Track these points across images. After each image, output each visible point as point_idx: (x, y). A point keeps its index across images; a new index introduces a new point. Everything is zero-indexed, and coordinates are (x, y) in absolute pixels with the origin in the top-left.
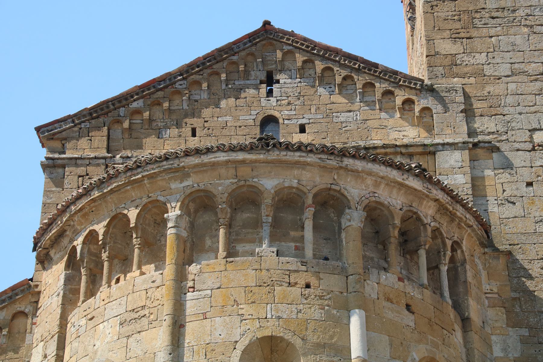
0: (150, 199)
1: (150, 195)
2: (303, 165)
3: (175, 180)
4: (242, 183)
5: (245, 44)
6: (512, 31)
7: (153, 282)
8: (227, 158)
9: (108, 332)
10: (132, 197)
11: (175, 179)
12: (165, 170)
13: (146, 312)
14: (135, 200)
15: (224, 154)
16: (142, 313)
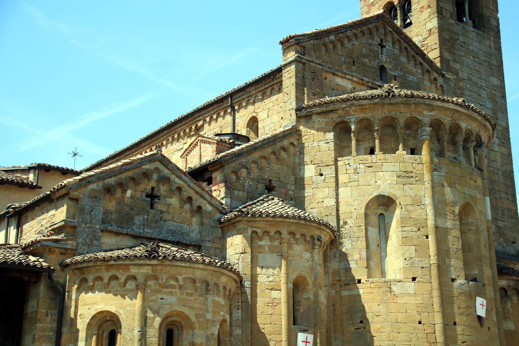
0: (411, 116)
1: (412, 113)
2: (475, 119)
3: (427, 110)
4: (454, 121)
5: (374, 20)
6: (468, 56)
7: (416, 160)
8: (454, 107)
9: (387, 178)
10: (401, 111)
11: (427, 110)
12: (426, 104)
13: (414, 175)
14: (403, 113)
15: (453, 105)
16: (411, 175)
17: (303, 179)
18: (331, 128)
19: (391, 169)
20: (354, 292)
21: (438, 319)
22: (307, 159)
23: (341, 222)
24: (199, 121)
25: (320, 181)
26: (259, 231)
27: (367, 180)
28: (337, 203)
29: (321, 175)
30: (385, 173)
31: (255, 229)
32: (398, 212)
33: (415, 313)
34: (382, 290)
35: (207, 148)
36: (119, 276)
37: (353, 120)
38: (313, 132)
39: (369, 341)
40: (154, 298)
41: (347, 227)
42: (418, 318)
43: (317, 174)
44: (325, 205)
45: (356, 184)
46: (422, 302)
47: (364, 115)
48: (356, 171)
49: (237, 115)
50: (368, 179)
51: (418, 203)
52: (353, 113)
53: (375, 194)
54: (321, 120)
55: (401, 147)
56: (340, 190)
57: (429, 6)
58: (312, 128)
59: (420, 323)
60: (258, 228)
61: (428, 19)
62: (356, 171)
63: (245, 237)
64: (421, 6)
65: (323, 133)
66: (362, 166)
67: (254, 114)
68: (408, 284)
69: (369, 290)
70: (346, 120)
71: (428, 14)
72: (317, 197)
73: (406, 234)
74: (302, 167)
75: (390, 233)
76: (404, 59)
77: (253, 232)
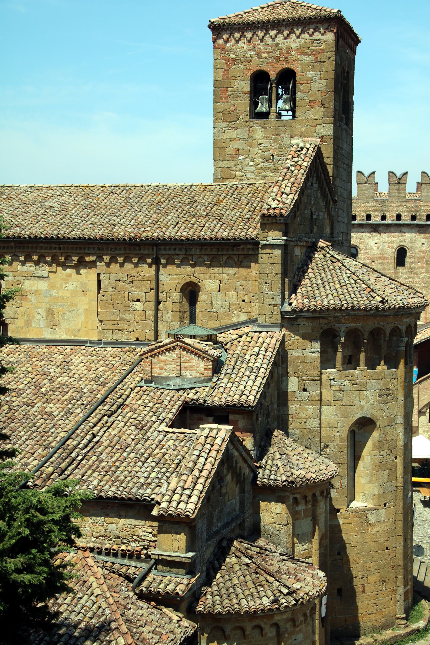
13: (391, 392)
17: (286, 394)
18: (318, 335)
19: (374, 386)
20: (334, 523)
21: (401, 544)
22: (290, 370)
23: (323, 444)
24: (93, 255)
25: (303, 399)
26: (298, 496)
27: (351, 399)
28: (320, 424)
29: (305, 390)
30: (368, 392)
31: (296, 496)
32: (375, 434)
33: (384, 540)
34: (359, 520)
35: (192, 359)
36: (263, 626)
37: (343, 329)
38: (297, 337)
39: (345, 572)
40: (290, 641)
41: (328, 450)
42: (386, 544)
43: (301, 389)
44: (308, 425)
45: (340, 403)
46: (389, 527)
47: (355, 325)
48: (341, 390)
49: (161, 269)
50: (353, 398)
51: (392, 423)
52: (344, 321)
53: (359, 416)
54: (307, 324)
55: (382, 362)
56: (324, 408)
57: (323, 105)
58: (296, 333)
59: (387, 549)
60: (297, 493)
61: (321, 122)
62: (341, 390)
63: (288, 507)
64: (311, 99)
65: (308, 342)
66: (347, 383)
67: (194, 279)
68: (381, 511)
69: (348, 520)
70: (335, 328)
71: (321, 115)
72: (300, 416)
73: (383, 459)
74: (284, 379)
75: (363, 453)
76: (319, 194)
77: (295, 499)
